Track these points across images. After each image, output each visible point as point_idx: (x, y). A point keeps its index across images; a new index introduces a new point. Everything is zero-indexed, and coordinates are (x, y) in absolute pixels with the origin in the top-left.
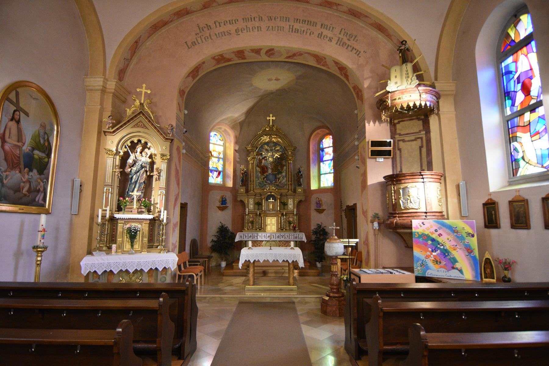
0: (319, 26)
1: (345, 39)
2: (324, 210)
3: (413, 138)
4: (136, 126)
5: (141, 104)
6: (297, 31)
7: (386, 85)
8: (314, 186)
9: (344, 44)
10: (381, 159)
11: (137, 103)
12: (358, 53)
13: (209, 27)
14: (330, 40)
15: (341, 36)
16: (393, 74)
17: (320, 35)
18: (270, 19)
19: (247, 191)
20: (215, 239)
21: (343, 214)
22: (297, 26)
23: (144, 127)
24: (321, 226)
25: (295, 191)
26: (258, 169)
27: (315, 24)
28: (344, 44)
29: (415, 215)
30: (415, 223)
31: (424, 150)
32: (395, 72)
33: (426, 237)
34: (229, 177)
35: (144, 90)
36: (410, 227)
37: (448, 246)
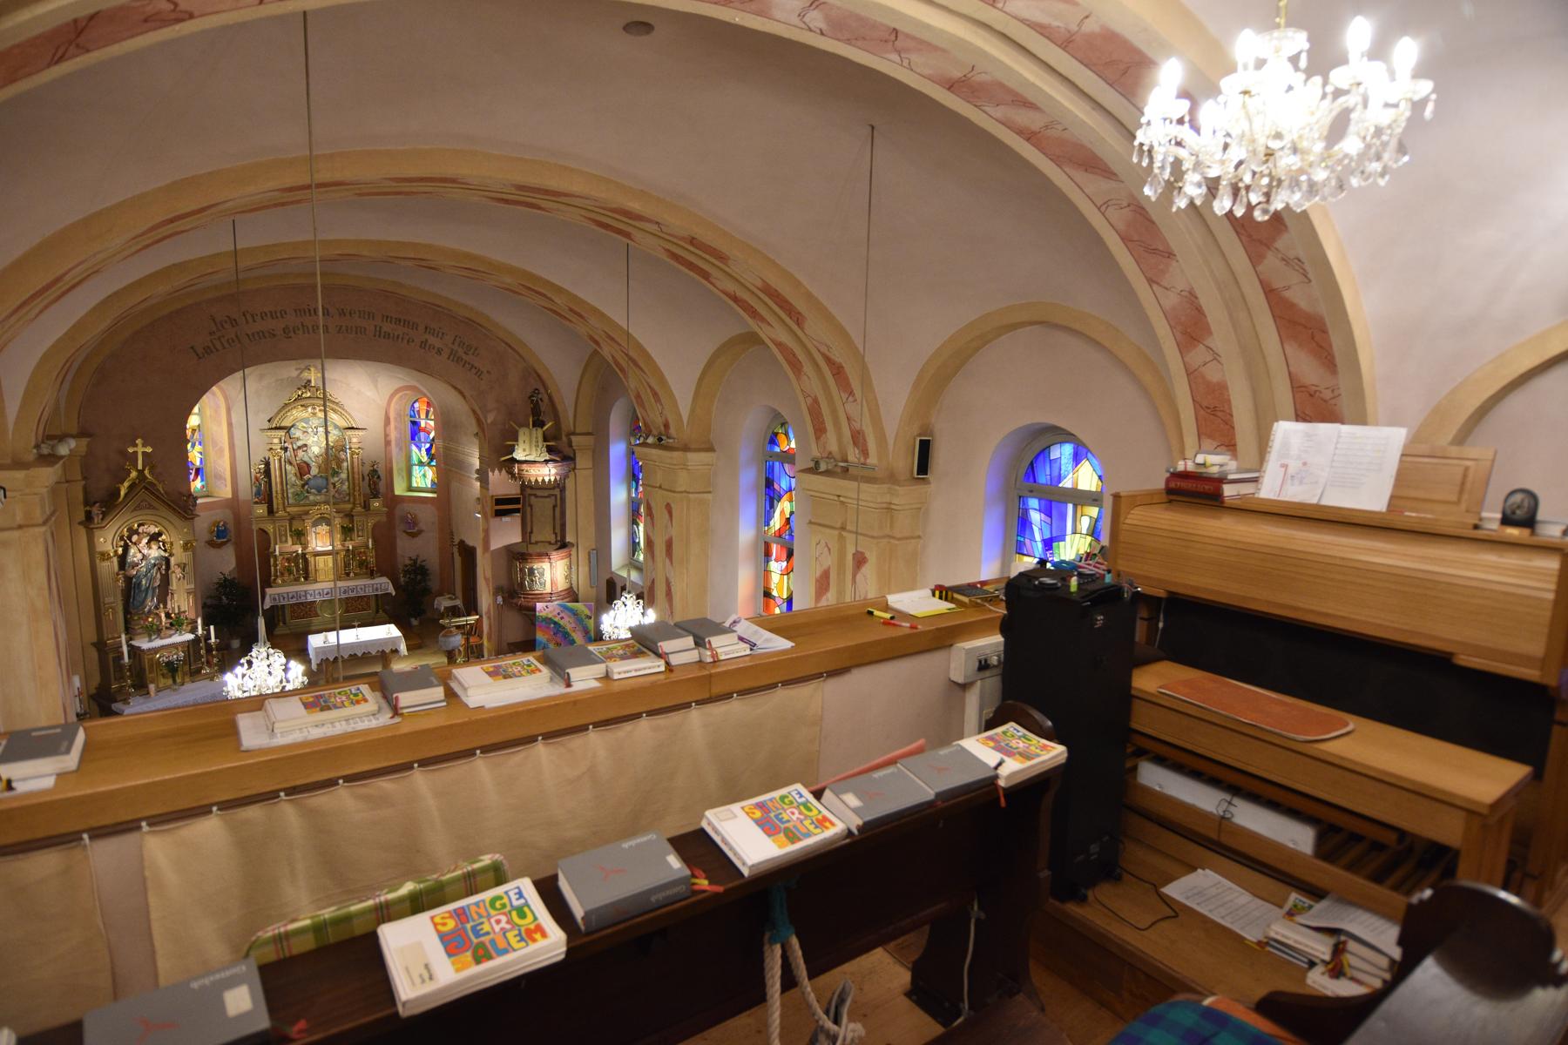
0: (422, 328)
1: (461, 352)
2: (420, 532)
3: (546, 493)
4: (138, 508)
5: (141, 472)
6: (387, 336)
7: (513, 451)
8: (399, 489)
9: (459, 360)
10: (506, 519)
11: (134, 474)
12: (479, 373)
13: (234, 322)
14: (439, 352)
15: (455, 347)
16: (521, 438)
17: (423, 344)
18: (342, 313)
19: (271, 511)
20: (209, 602)
21: (455, 550)
22: (387, 327)
23: (150, 507)
24: (415, 561)
25: (366, 506)
26: (289, 467)
27: (415, 326)
28: (459, 360)
29: (541, 597)
30: (539, 606)
31: (558, 510)
32: (523, 435)
33: (548, 620)
34: (219, 477)
35: (140, 450)
36: (534, 609)
37: (569, 628)
